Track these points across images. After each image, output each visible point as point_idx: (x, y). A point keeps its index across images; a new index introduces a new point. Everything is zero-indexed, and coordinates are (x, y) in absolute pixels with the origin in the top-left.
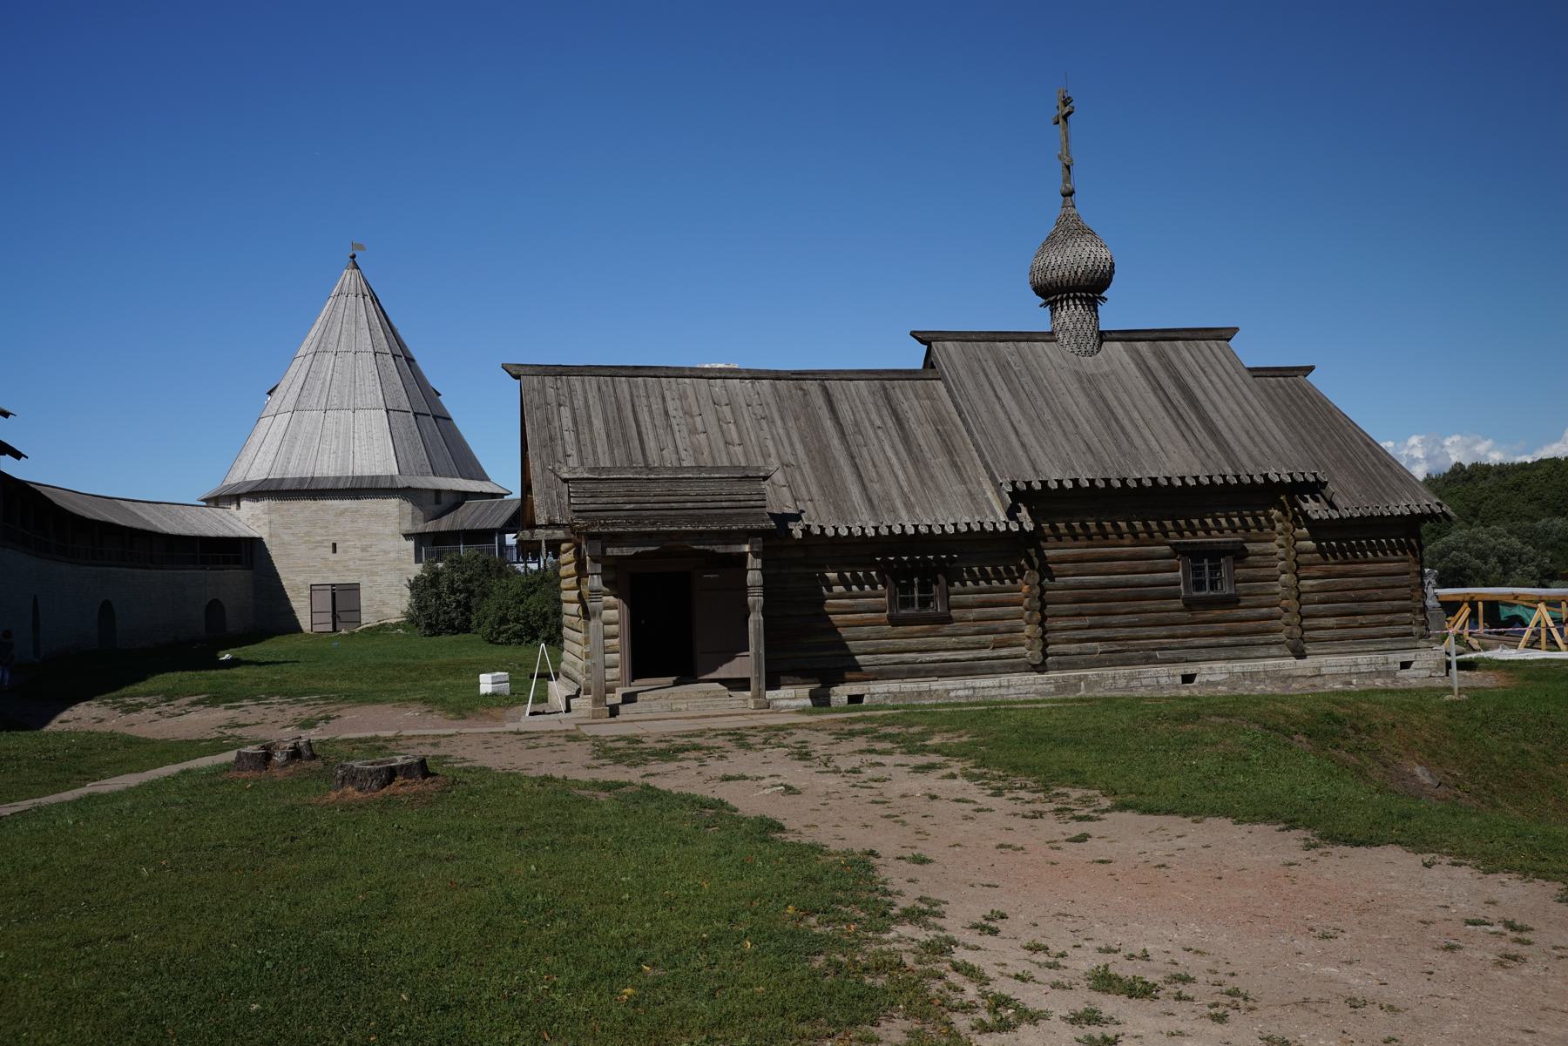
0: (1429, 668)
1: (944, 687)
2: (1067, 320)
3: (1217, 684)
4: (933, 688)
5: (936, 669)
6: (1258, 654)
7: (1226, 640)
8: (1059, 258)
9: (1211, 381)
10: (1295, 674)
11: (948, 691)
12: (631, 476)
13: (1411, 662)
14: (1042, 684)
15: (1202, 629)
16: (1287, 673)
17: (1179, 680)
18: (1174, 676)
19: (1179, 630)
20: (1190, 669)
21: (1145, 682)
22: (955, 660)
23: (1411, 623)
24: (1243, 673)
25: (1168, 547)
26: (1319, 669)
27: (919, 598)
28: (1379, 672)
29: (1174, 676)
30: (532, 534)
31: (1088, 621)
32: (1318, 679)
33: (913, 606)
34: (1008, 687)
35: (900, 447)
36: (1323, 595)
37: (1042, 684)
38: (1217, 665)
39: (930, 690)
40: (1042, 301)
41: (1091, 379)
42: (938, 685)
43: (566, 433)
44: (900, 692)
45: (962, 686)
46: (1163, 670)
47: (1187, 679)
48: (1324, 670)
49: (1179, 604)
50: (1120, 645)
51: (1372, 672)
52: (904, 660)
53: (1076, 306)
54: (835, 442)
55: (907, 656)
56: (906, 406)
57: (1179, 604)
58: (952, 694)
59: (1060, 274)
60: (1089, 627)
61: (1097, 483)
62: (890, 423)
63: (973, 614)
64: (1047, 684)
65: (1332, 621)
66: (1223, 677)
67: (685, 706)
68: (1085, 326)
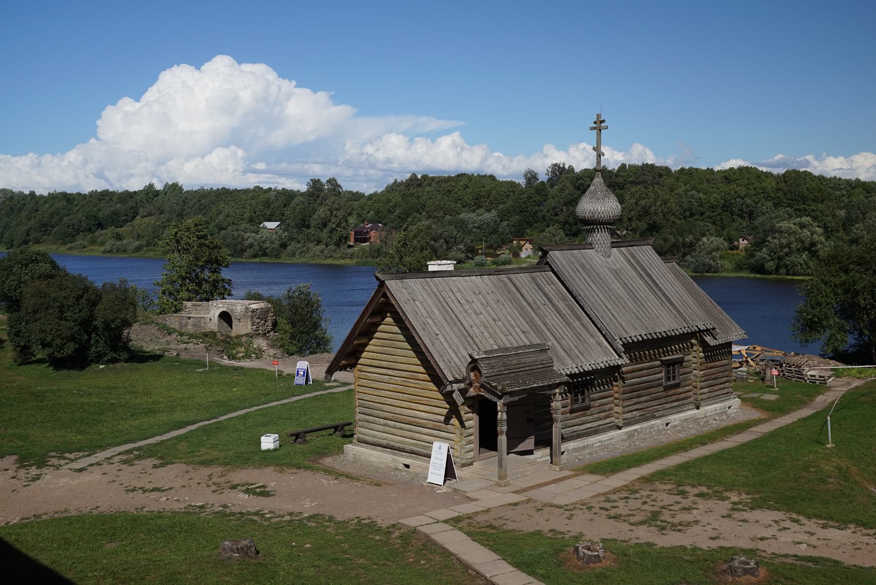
2: (600, 238)
5: (585, 433)
6: (686, 409)
7: (676, 404)
8: (602, 208)
11: (593, 444)
12: (500, 354)
15: (669, 399)
19: (662, 401)
25: (659, 362)
26: (706, 414)
30: (452, 387)
31: (635, 400)
35: (558, 316)
36: (704, 378)
43: (427, 319)
48: (707, 415)
49: (661, 389)
50: (644, 412)
53: (605, 231)
54: (534, 315)
56: (546, 290)
57: (661, 389)
59: (603, 216)
60: (635, 404)
62: (548, 303)
66: (678, 422)
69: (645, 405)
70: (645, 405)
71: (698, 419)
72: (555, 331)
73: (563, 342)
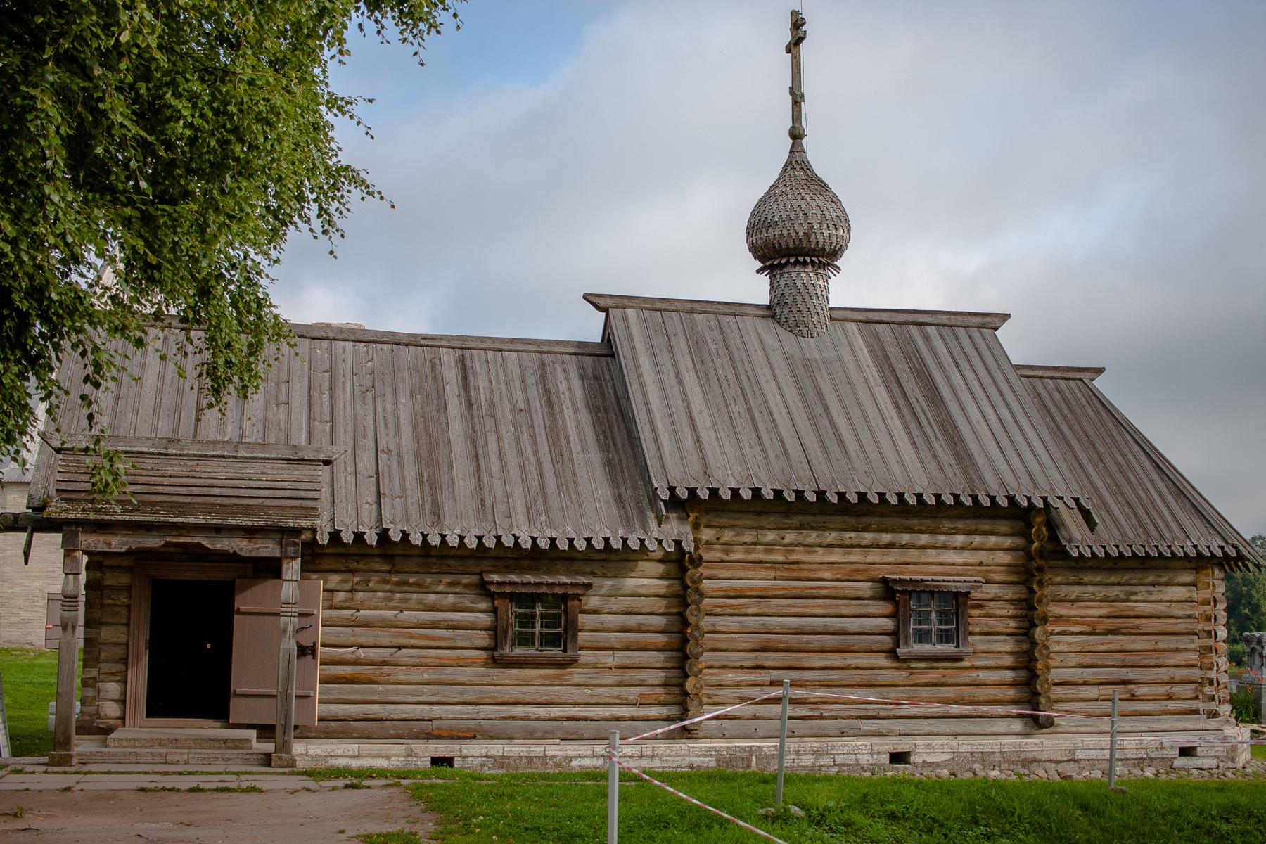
0: (1215, 757)
1: (564, 753)
3: (937, 765)
4: (549, 753)
6: (995, 729)
7: (954, 709)
9: (964, 377)
10: (1040, 757)
11: (569, 759)
13: (1195, 748)
14: (698, 756)
16: (1030, 756)
17: (885, 759)
18: (879, 753)
19: (893, 694)
20: (902, 745)
21: (839, 759)
22: (586, 719)
23: (1197, 698)
24: (972, 753)
27: (541, 633)
28: (1151, 759)
29: (879, 753)
32: (1072, 764)
33: (533, 644)
34: (653, 757)
37: (698, 756)
38: (937, 742)
39: (545, 756)
40: (760, 265)
41: (807, 364)
42: (555, 749)
44: (503, 757)
45: (589, 753)
46: (864, 744)
47: (898, 758)
48: (1080, 755)
50: (812, 709)
51: (1142, 759)
52: (514, 714)
55: (519, 710)
58: (575, 763)
59: (777, 232)
61: (785, 494)
63: (609, 659)
64: (705, 756)
65: (1093, 692)
67: (185, 757)
68: (807, 298)
69: (817, 694)
70: (817, 694)
71: (1034, 761)
72: (494, 458)
73: (498, 484)
